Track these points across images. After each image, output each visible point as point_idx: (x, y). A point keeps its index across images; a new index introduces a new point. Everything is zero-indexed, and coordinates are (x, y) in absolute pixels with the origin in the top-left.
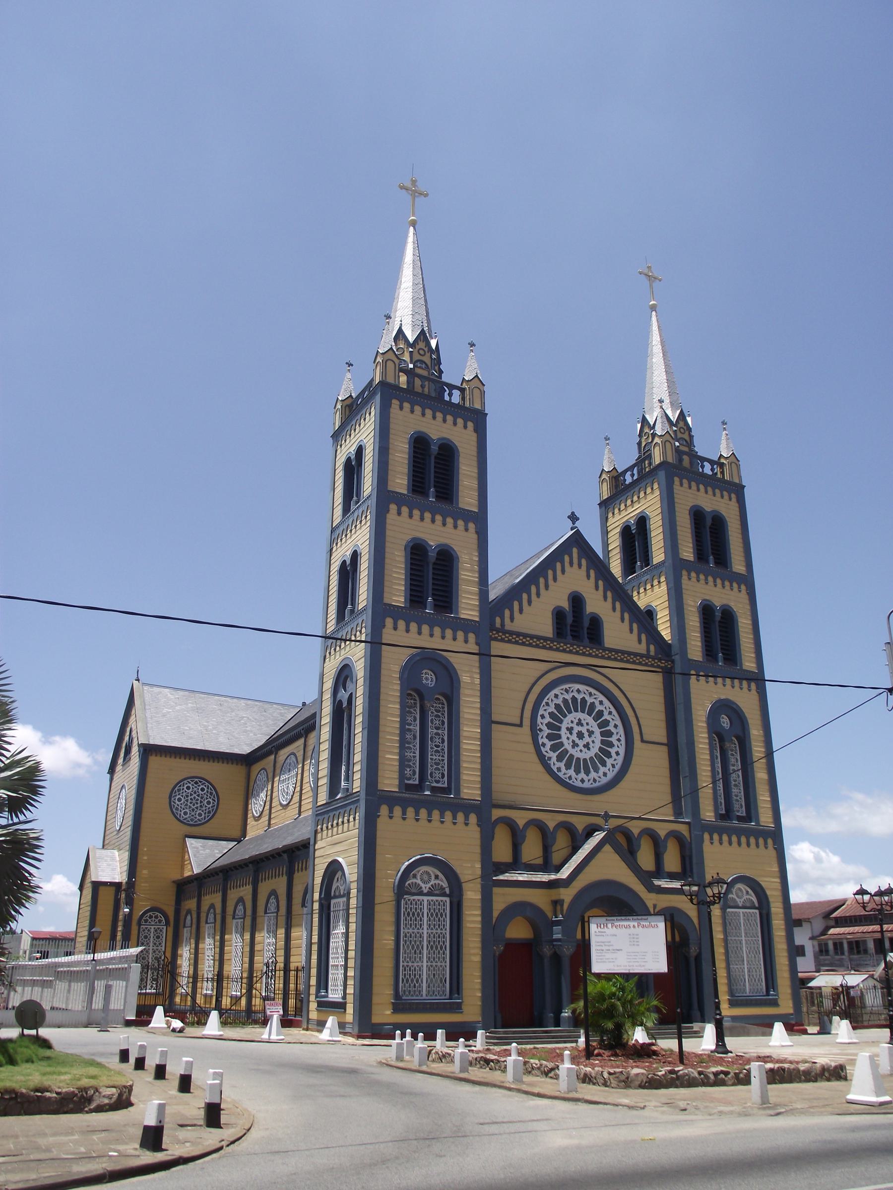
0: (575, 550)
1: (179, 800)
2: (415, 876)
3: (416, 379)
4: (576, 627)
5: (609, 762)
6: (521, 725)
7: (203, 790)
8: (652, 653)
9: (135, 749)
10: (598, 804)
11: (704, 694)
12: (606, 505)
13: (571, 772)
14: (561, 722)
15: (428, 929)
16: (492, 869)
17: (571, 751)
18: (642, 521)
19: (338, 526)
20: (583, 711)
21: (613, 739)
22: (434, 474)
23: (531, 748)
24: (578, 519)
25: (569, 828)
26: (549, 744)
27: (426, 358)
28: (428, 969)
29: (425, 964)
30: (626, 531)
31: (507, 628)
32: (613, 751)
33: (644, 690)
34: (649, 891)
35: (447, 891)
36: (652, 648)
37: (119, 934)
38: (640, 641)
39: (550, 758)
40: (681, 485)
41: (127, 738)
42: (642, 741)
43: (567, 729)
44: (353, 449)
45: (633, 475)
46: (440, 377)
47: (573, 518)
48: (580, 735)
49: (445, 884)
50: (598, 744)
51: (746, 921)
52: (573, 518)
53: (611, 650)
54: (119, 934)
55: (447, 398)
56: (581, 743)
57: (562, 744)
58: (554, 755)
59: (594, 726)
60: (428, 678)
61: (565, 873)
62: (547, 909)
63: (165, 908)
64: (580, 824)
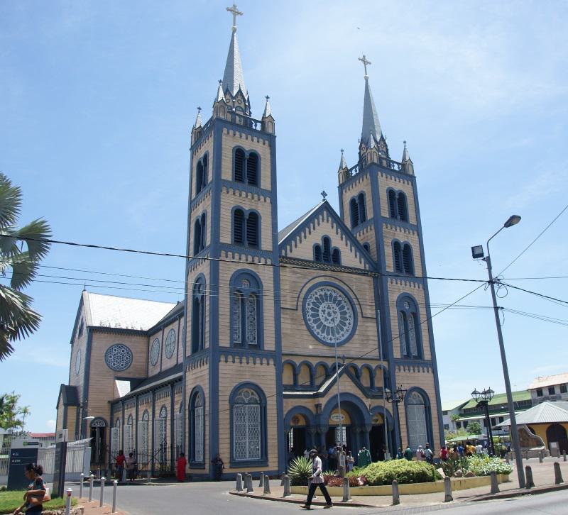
0: (325, 212)
1: (111, 357)
2: (240, 394)
3: (237, 117)
4: (326, 255)
5: (345, 328)
6: (297, 310)
7: (123, 351)
8: (367, 269)
9: (85, 328)
10: (339, 352)
11: (396, 289)
12: (341, 188)
13: (325, 334)
14: (319, 307)
15: (248, 422)
16: (281, 387)
17: (325, 323)
18: (362, 196)
19: (195, 199)
21: (347, 316)
22: (248, 169)
24: (326, 195)
25: (324, 365)
26: (312, 319)
27: (242, 106)
28: (250, 446)
29: (247, 441)
30: (353, 202)
31: (289, 255)
32: (347, 322)
33: (363, 288)
34: (367, 397)
35: (259, 402)
36: (367, 266)
37: (80, 432)
38: (361, 262)
39: (313, 327)
40: (382, 176)
41: (80, 321)
42: (363, 317)
43: (322, 311)
44: (202, 155)
45: (356, 171)
46: (250, 116)
47: (324, 194)
48: (329, 314)
49: (258, 399)
50: (339, 319)
51: (418, 413)
52: (324, 194)
53: (345, 267)
54: (80, 432)
55: (254, 127)
57: (319, 319)
58: (315, 325)
60: (245, 286)
61: (322, 390)
62: (313, 409)
63: (104, 417)
64: (330, 363)
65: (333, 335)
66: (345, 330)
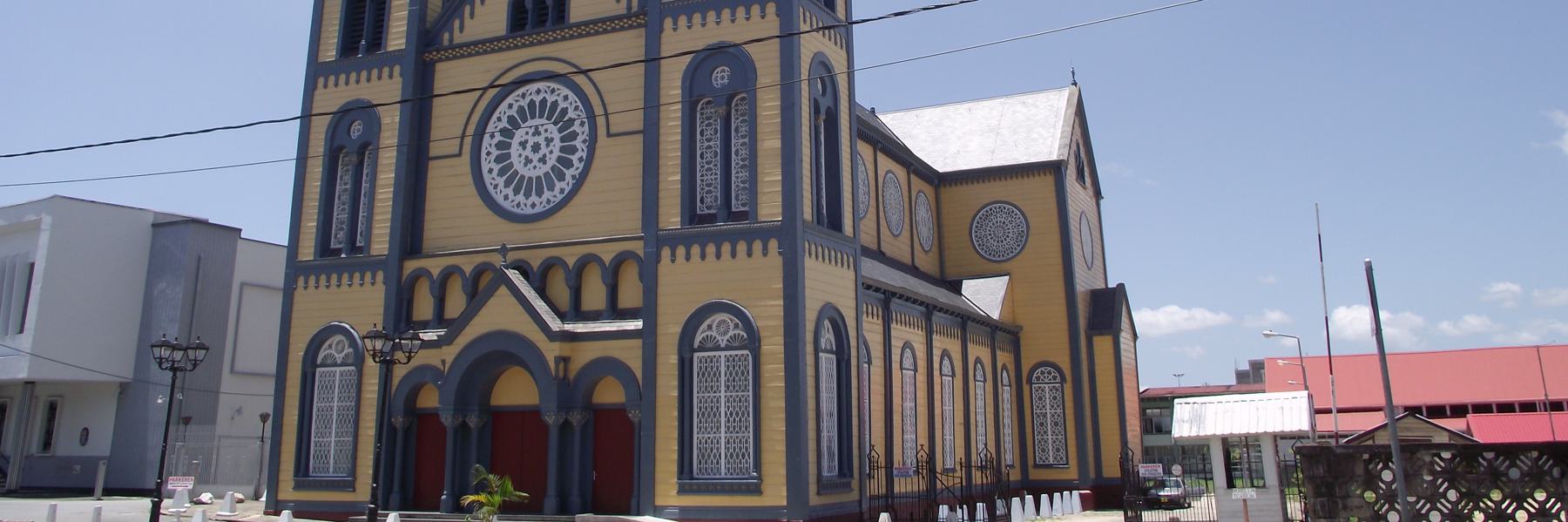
5: (524, 103)
14: (546, 174)
17: (557, 136)
20: (516, 172)
23: (596, 163)
26: (575, 158)
32: (513, 112)
48: (536, 148)
56: (541, 140)
57: (562, 150)
58: (578, 143)
59: (515, 150)
65: (555, 104)
66: (528, 100)
